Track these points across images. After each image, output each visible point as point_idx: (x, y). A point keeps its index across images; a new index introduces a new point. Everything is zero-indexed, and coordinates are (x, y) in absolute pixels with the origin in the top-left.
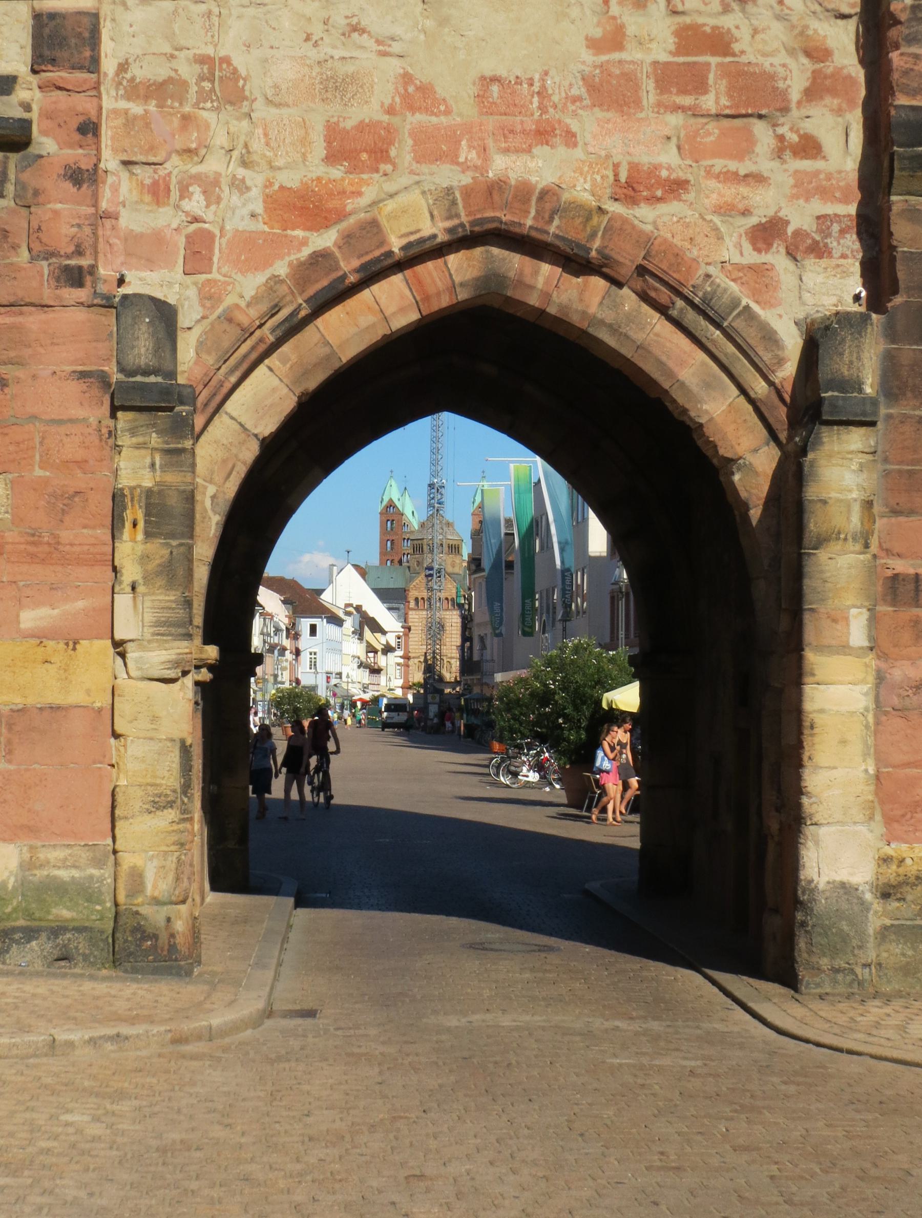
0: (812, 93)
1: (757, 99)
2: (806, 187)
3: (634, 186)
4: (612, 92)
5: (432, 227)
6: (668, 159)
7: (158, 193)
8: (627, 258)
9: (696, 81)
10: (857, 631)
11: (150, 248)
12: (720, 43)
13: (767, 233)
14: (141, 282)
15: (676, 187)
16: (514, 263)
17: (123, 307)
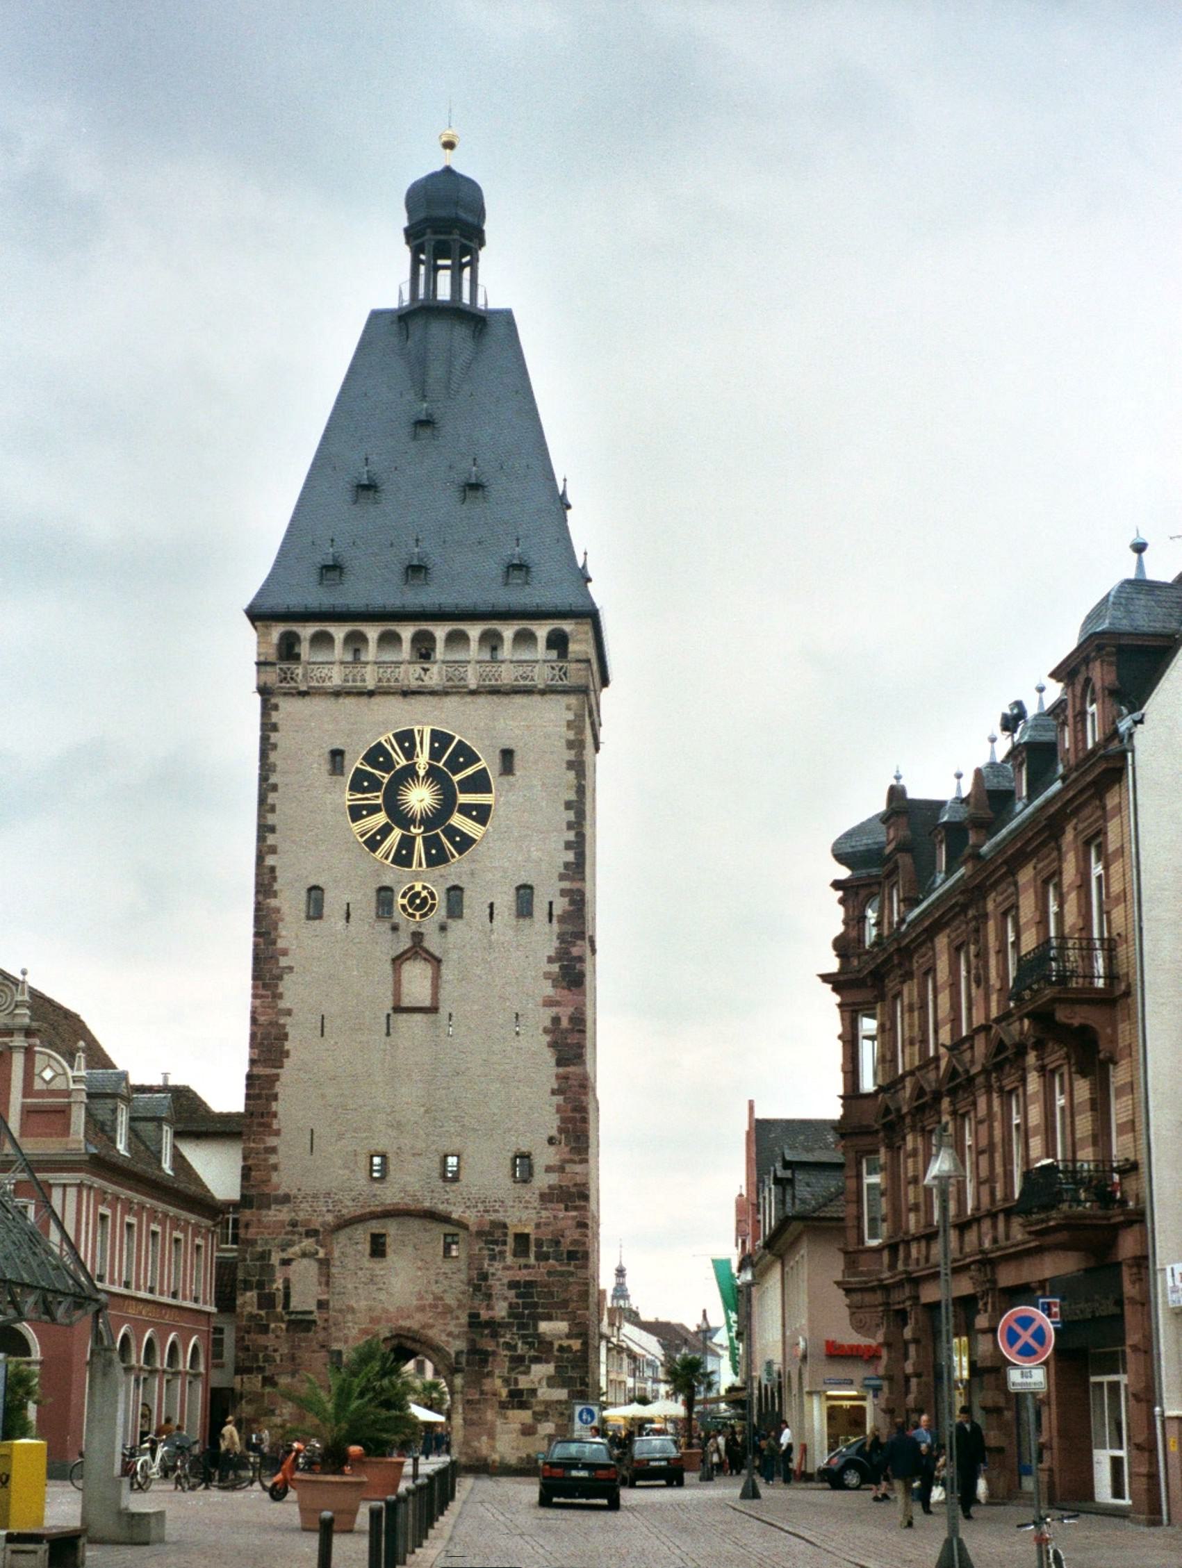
0: (459, 1307)
1: (448, 1310)
2: (456, 1326)
3: (426, 1326)
4: (421, 1309)
5: (388, 1335)
6: (431, 1321)
7: (340, 1330)
8: (423, 1339)
9: (436, 1306)
10: (460, 1410)
11: (337, 1340)
12: (441, 1299)
13: (450, 1334)
14: (336, 1346)
15: (432, 1326)
16: (403, 1340)
17: (332, 1352)
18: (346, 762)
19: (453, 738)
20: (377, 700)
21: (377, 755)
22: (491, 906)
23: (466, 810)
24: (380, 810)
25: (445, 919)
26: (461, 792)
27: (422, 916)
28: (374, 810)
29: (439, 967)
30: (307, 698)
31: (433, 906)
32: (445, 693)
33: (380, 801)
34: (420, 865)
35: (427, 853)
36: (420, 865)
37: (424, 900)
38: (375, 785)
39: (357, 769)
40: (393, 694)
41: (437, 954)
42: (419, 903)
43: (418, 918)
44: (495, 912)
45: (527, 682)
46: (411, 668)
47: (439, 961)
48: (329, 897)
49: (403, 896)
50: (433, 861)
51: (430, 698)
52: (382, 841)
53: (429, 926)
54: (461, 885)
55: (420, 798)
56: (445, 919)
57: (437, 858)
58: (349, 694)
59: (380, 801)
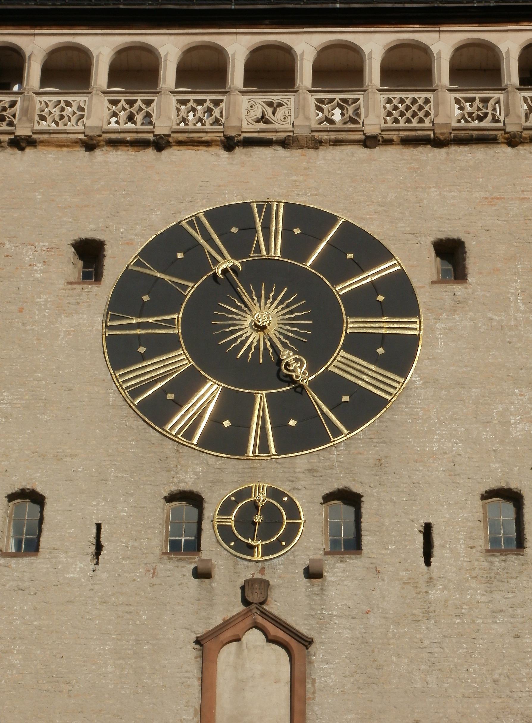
18: (108, 263)
19: (334, 219)
20: (173, 155)
21: (172, 248)
22: (427, 531)
23: (361, 345)
24: (178, 346)
25: (319, 555)
26: (350, 314)
27: (268, 550)
28: (163, 345)
29: (307, 661)
30: (29, 151)
31: (293, 530)
32: (316, 144)
33: (177, 330)
34: (264, 448)
35: (280, 427)
36: (264, 448)
37: (270, 511)
38: (167, 300)
39: (128, 274)
40: (207, 144)
41: (304, 629)
42: (262, 523)
43: (258, 555)
44: (437, 541)
45: (486, 123)
46: (244, 101)
47: (307, 642)
48: (50, 510)
49: (226, 508)
50: (289, 442)
51: (281, 151)
52: (178, 404)
53: (284, 573)
54: (356, 488)
55: (262, 321)
56: (319, 555)
57: (301, 433)
58: (114, 143)
59: (177, 330)
